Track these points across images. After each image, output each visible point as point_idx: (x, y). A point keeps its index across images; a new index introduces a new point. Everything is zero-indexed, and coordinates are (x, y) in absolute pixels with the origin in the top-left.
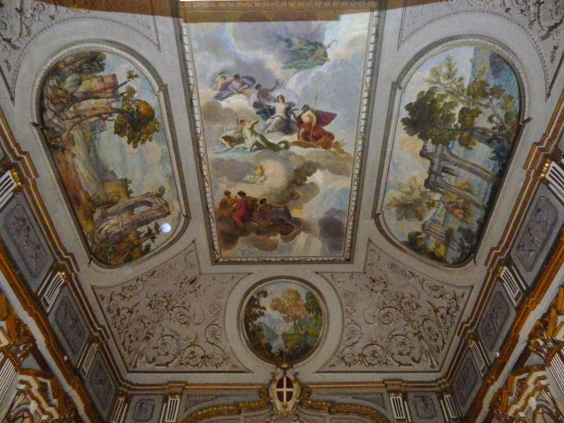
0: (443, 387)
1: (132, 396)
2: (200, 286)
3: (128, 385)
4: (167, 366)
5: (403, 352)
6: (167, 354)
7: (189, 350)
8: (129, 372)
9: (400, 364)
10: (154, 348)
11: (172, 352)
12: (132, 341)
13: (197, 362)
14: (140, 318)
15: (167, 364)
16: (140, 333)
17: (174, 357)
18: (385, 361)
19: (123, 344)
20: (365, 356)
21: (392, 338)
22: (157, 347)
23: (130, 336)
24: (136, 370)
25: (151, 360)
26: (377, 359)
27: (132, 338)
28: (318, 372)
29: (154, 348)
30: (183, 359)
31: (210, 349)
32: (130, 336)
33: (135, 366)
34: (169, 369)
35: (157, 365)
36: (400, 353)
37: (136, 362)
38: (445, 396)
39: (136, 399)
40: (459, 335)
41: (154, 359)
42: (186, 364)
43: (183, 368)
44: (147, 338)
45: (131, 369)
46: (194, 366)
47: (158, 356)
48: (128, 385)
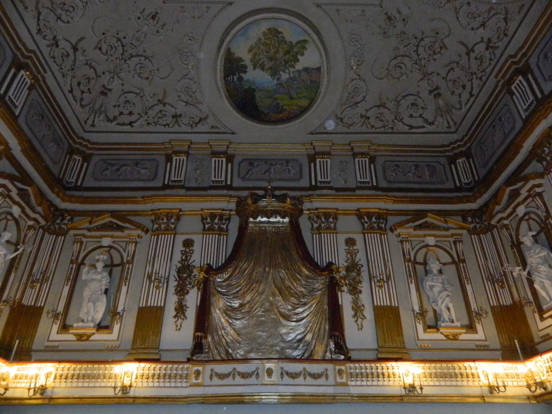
0: (457, 151)
1: (92, 155)
2: (165, 24)
3: (84, 143)
4: (132, 126)
5: (414, 114)
6: (131, 113)
7: (157, 109)
8: (86, 132)
9: (411, 127)
10: (115, 106)
11: (136, 111)
12: (83, 92)
13: (168, 122)
14: (89, 62)
15: (131, 124)
16: (93, 82)
17: (139, 116)
18: (390, 126)
19: (71, 91)
20: (368, 118)
21: (401, 99)
22: (119, 106)
23: (79, 84)
24: (96, 129)
25: (112, 118)
26: (382, 123)
27: (82, 87)
28: (312, 134)
29: (115, 106)
30: (151, 118)
31: (181, 108)
32: (79, 84)
33: (93, 125)
34: (133, 129)
35: (118, 124)
36: (411, 116)
37: (94, 121)
38: (457, 161)
39: (95, 159)
40: (496, 77)
41: (115, 118)
42: (154, 124)
43: (151, 128)
44: (104, 93)
45: (87, 128)
46: (165, 126)
47: (120, 115)
48: (84, 143)
